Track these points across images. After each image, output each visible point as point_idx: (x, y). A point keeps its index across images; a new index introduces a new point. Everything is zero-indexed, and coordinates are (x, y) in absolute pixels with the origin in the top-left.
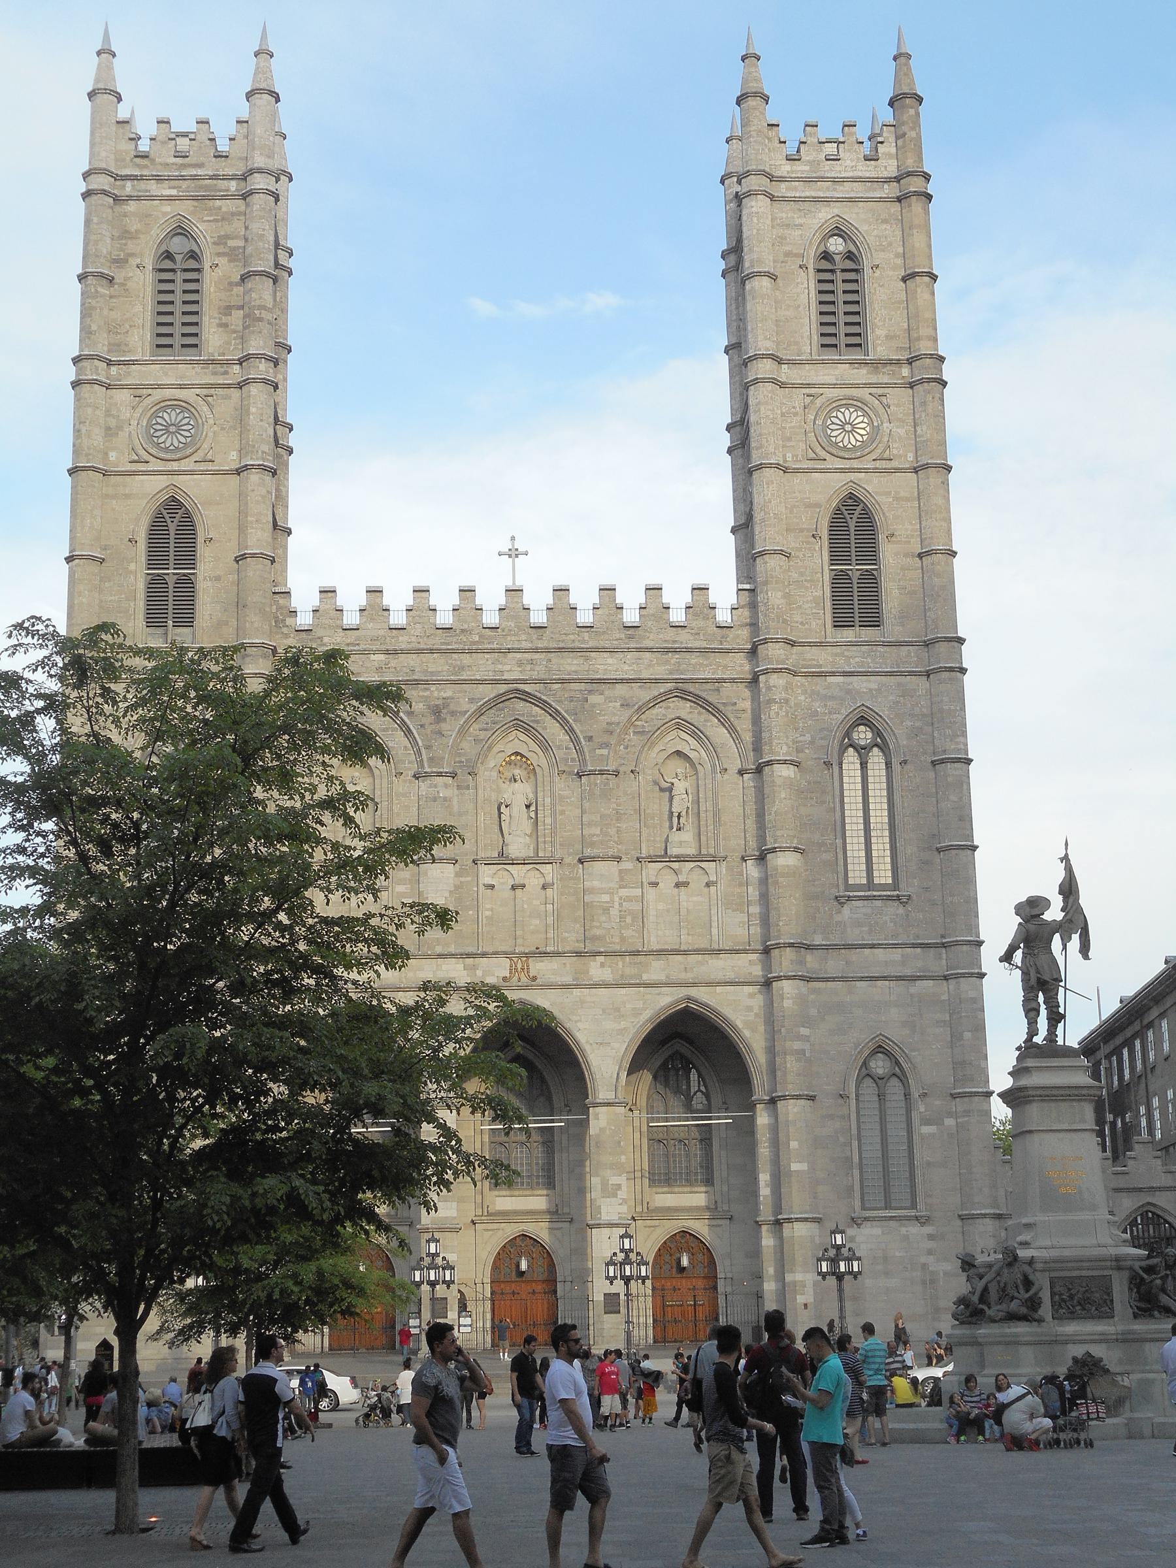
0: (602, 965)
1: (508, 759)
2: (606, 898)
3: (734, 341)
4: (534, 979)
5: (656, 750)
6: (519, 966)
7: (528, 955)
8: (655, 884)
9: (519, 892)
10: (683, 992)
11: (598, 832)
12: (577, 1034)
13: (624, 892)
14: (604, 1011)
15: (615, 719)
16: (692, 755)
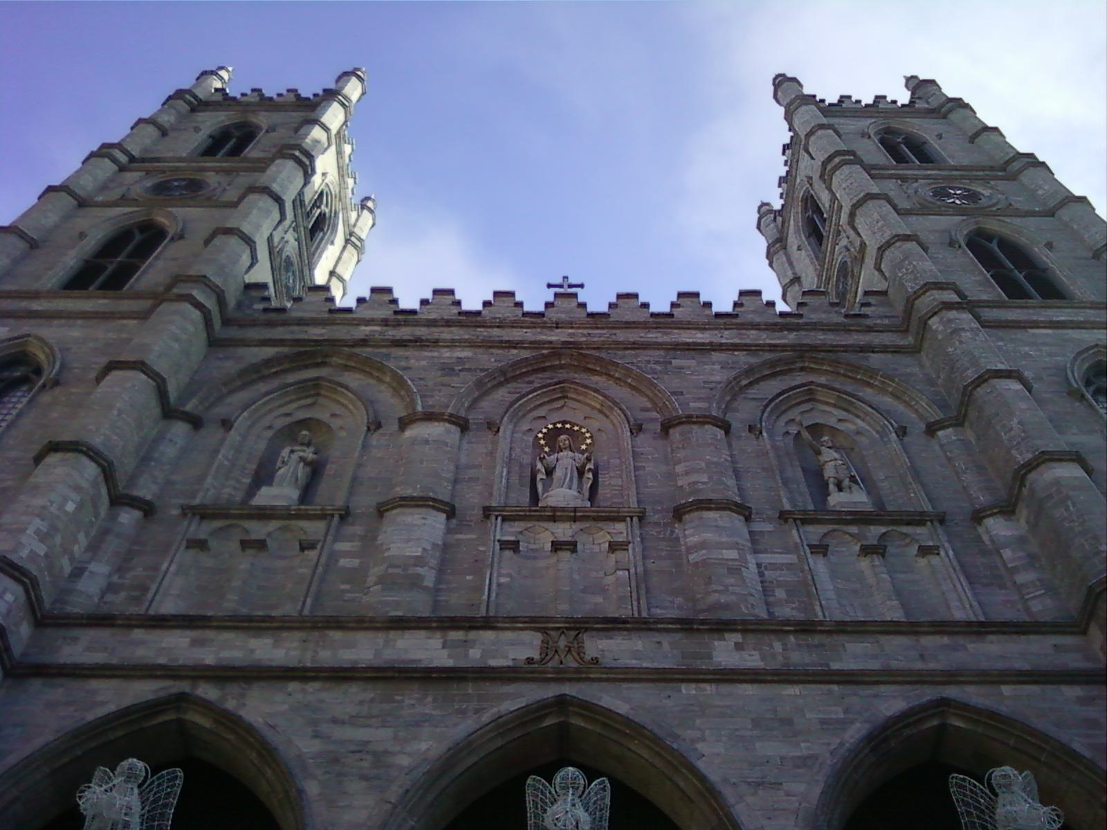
0: (739, 647)
1: (550, 426)
2: (733, 554)
3: (790, 275)
4: (595, 661)
5: (785, 418)
6: (562, 643)
7: (580, 626)
8: (820, 549)
9: (565, 555)
10: (929, 693)
11: (705, 480)
12: (701, 765)
13: (766, 558)
14: (756, 723)
15: (718, 378)
16: (841, 426)
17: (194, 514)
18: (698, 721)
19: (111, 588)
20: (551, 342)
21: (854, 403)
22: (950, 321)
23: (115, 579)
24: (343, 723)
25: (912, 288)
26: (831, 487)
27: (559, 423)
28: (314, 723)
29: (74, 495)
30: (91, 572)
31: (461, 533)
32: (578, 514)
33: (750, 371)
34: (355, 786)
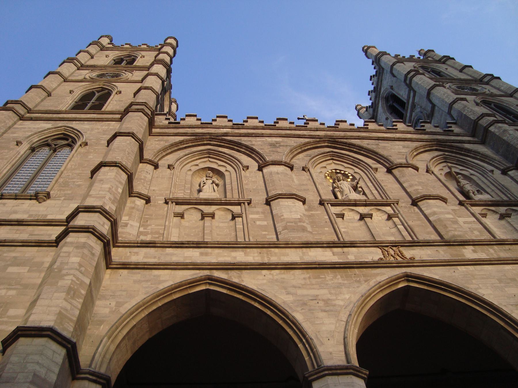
0: (474, 251)
14: (500, 281)
17: (172, 202)
18: (474, 281)
19: (140, 233)
20: (319, 136)
21: (465, 162)
22: (500, 127)
23: (141, 229)
24: (300, 288)
25: (473, 117)
26: (471, 194)
27: (334, 170)
28: (285, 288)
29: (119, 185)
30: (131, 225)
31: (312, 211)
32: (367, 202)
33: (416, 149)
34: (321, 315)
